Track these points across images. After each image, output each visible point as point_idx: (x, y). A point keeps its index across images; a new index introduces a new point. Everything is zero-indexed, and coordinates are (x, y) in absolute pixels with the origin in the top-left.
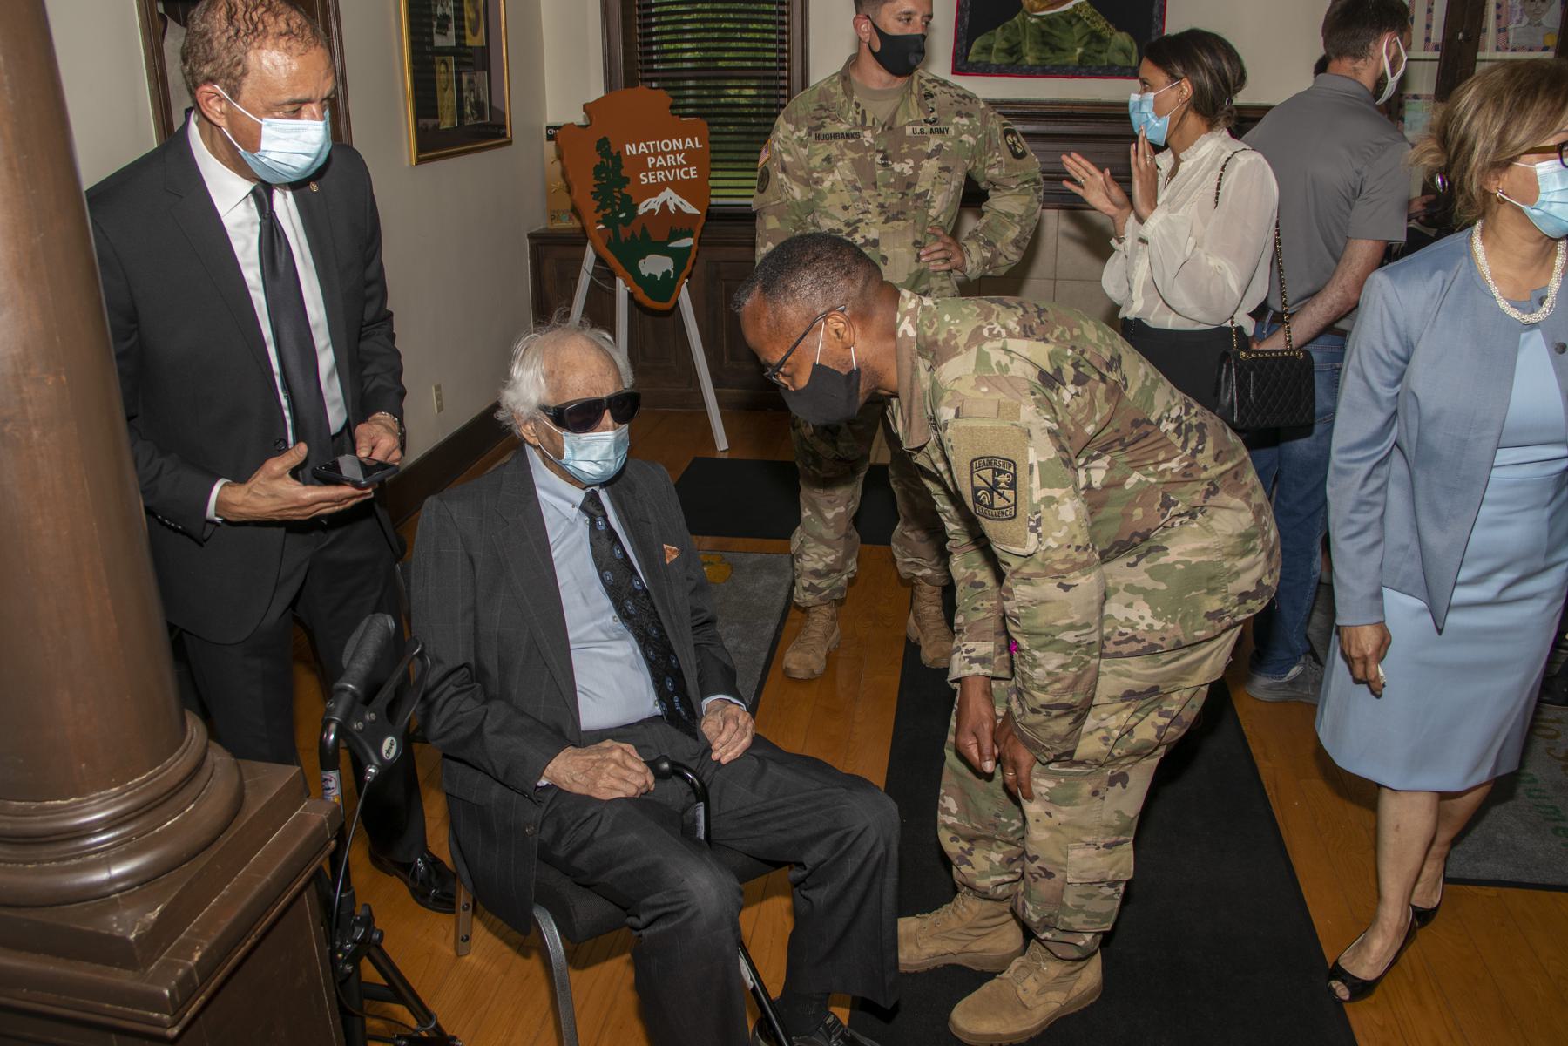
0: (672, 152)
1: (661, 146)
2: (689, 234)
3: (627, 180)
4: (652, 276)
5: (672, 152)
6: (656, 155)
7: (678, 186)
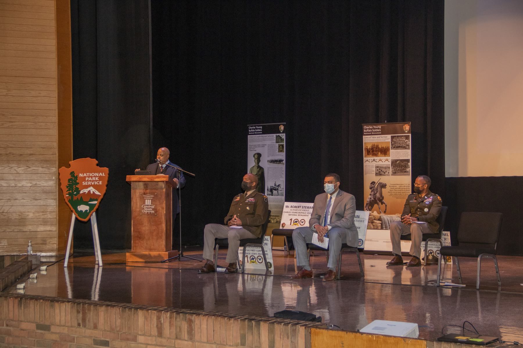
0: (95, 176)
1: (91, 175)
2: (96, 200)
3: (78, 183)
4: (81, 211)
5: (95, 176)
6: (89, 177)
7: (95, 186)
